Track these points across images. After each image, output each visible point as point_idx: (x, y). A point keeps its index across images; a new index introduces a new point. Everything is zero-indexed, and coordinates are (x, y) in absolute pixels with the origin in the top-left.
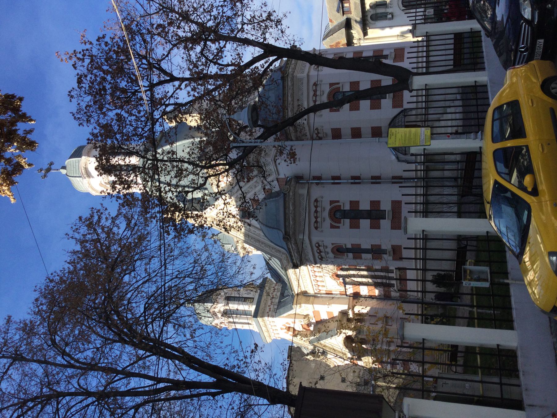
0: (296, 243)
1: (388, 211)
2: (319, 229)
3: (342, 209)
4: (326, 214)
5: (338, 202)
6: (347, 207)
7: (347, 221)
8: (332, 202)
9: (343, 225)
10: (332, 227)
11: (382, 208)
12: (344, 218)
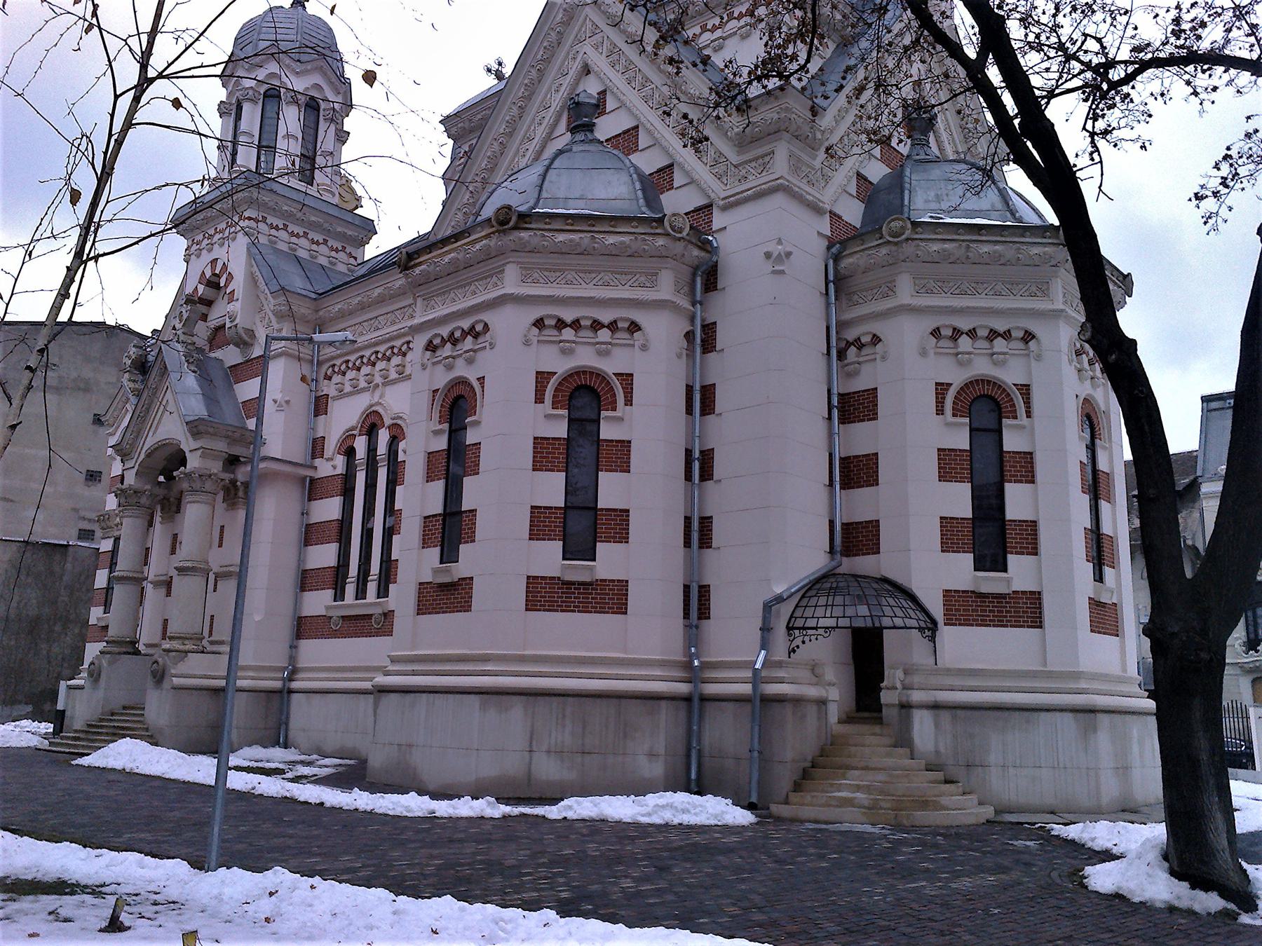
0: (487, 256)
1: (591, 568)
3: (604, 413)
4: (585, 358)
5: (629, 401)
6: (607, 432)
7: (560, 430)
8: (627, 379)
9: (547, 416)
10: (542, 378)
11: (603, 549)
12: (571, 421)
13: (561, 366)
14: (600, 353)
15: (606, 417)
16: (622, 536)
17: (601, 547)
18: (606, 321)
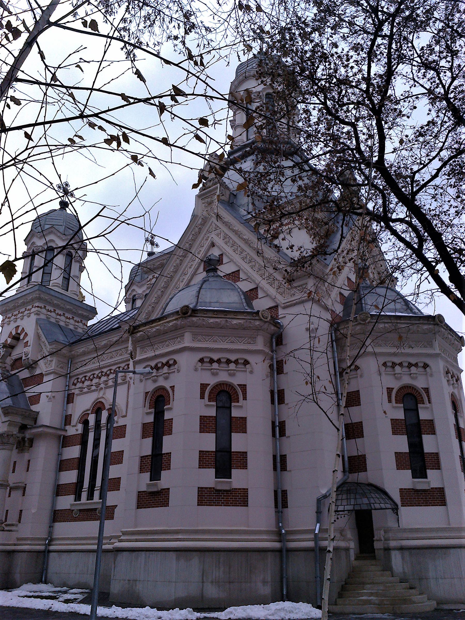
0: (176, 328)
1: (230, 483)
2: (200, 364)
3: (233, 404)
4: (223, 377)
5: (245, 398)
6: (235, 413)
7: (212, 412)
8: (243, 387)
9: (207, 406)
10: (203, 387)
13: (212, 381)
14: (230, 375)
15: (235, 406)
16: (244, 466)
17: (234, 472)
18: (233, 360)
